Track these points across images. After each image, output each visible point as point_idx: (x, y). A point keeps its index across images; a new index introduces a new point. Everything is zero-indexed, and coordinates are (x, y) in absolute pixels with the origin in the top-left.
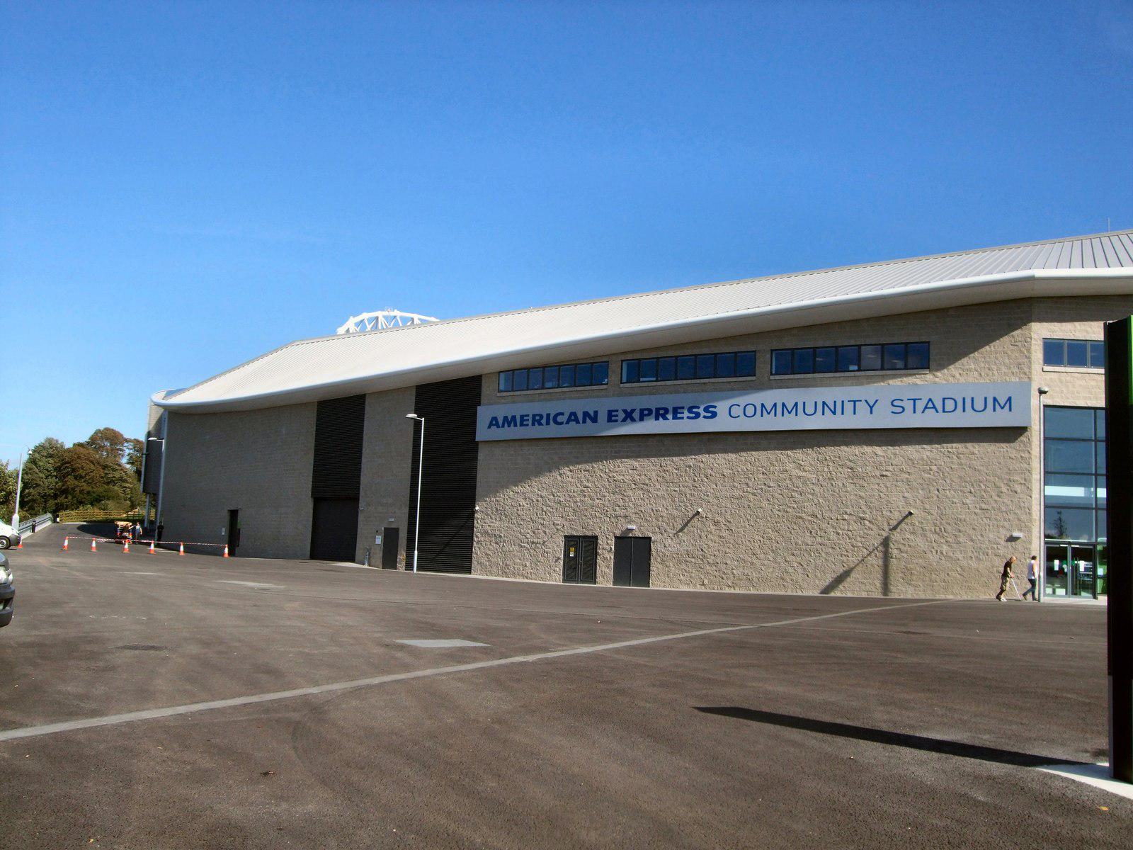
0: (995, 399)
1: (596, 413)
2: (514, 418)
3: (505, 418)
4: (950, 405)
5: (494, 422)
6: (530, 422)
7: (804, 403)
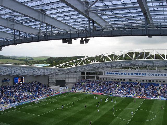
2: (111, 73)
3: (110, 73)
5: (108, 73)
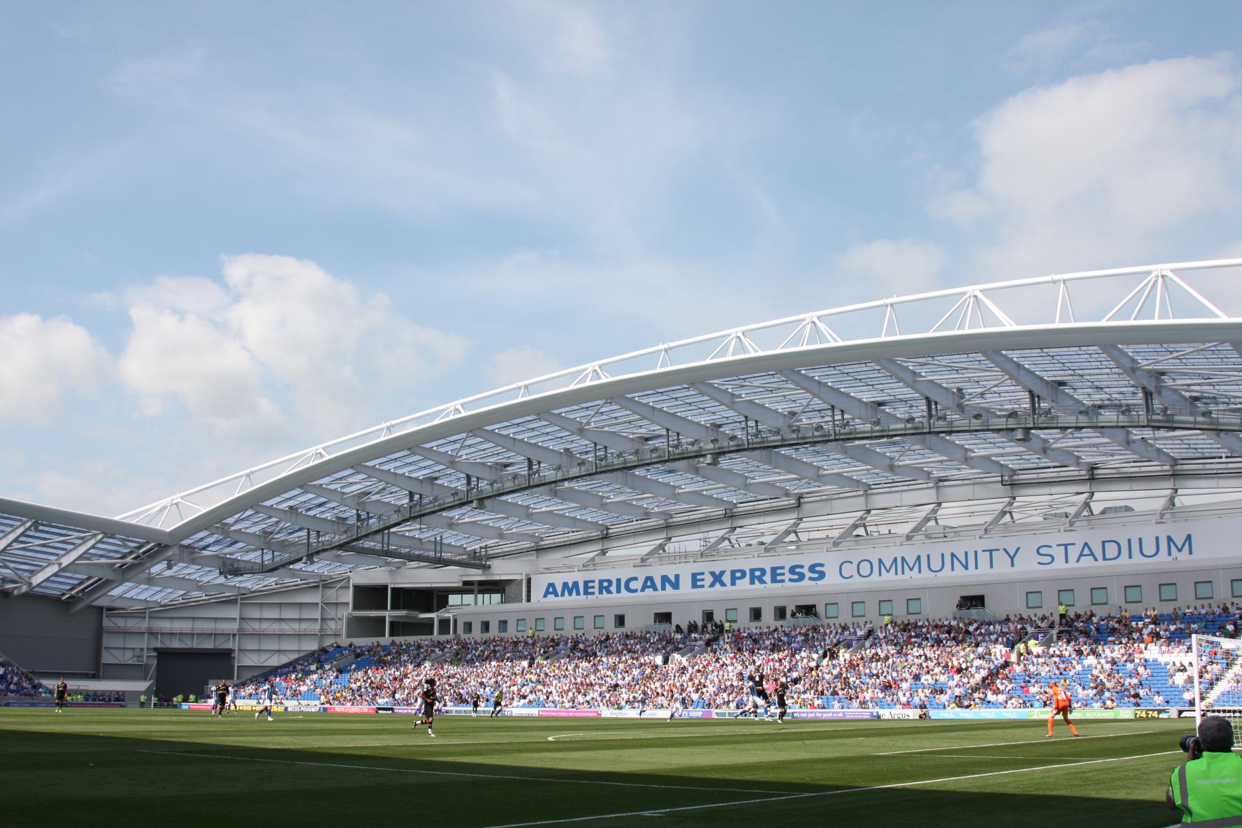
0: (1169, 539)
1: (677, 577)
2: (576, 584)
3: (565, 585)
4: (1111, 550)
5: (551, 589)
6: (596, 590)
7: (928, 556)
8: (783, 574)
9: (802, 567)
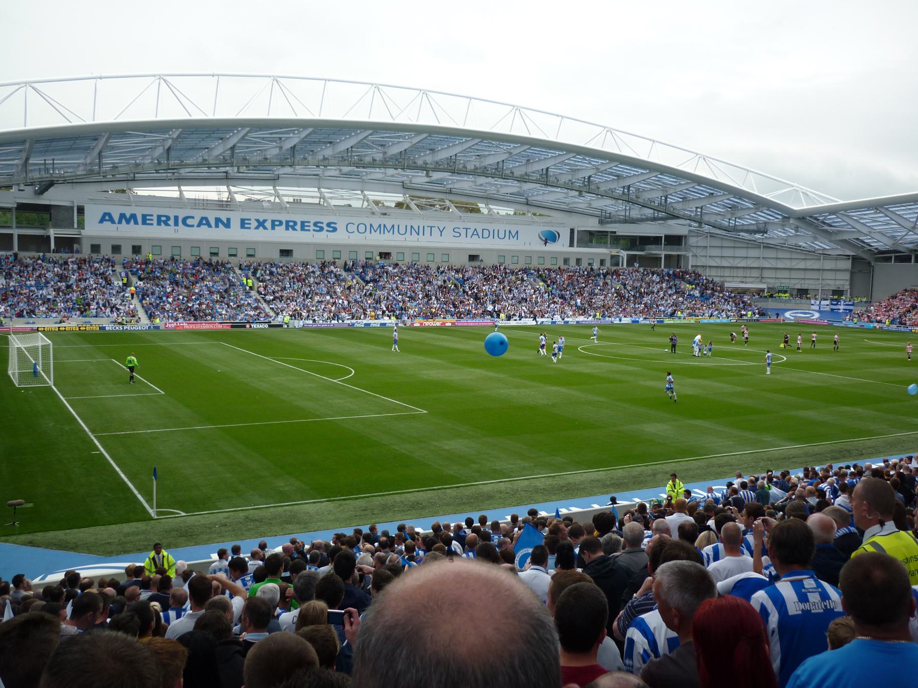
0: (510, 231)
1: (229, 220)
2: (133, 216)
3: (122, 216)
4: (486, 234)
5: (106, 217)
6: (155, 222)
8: (309, 226)
9: (322, 223)
